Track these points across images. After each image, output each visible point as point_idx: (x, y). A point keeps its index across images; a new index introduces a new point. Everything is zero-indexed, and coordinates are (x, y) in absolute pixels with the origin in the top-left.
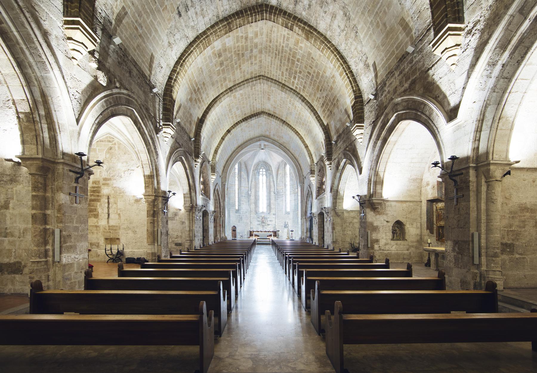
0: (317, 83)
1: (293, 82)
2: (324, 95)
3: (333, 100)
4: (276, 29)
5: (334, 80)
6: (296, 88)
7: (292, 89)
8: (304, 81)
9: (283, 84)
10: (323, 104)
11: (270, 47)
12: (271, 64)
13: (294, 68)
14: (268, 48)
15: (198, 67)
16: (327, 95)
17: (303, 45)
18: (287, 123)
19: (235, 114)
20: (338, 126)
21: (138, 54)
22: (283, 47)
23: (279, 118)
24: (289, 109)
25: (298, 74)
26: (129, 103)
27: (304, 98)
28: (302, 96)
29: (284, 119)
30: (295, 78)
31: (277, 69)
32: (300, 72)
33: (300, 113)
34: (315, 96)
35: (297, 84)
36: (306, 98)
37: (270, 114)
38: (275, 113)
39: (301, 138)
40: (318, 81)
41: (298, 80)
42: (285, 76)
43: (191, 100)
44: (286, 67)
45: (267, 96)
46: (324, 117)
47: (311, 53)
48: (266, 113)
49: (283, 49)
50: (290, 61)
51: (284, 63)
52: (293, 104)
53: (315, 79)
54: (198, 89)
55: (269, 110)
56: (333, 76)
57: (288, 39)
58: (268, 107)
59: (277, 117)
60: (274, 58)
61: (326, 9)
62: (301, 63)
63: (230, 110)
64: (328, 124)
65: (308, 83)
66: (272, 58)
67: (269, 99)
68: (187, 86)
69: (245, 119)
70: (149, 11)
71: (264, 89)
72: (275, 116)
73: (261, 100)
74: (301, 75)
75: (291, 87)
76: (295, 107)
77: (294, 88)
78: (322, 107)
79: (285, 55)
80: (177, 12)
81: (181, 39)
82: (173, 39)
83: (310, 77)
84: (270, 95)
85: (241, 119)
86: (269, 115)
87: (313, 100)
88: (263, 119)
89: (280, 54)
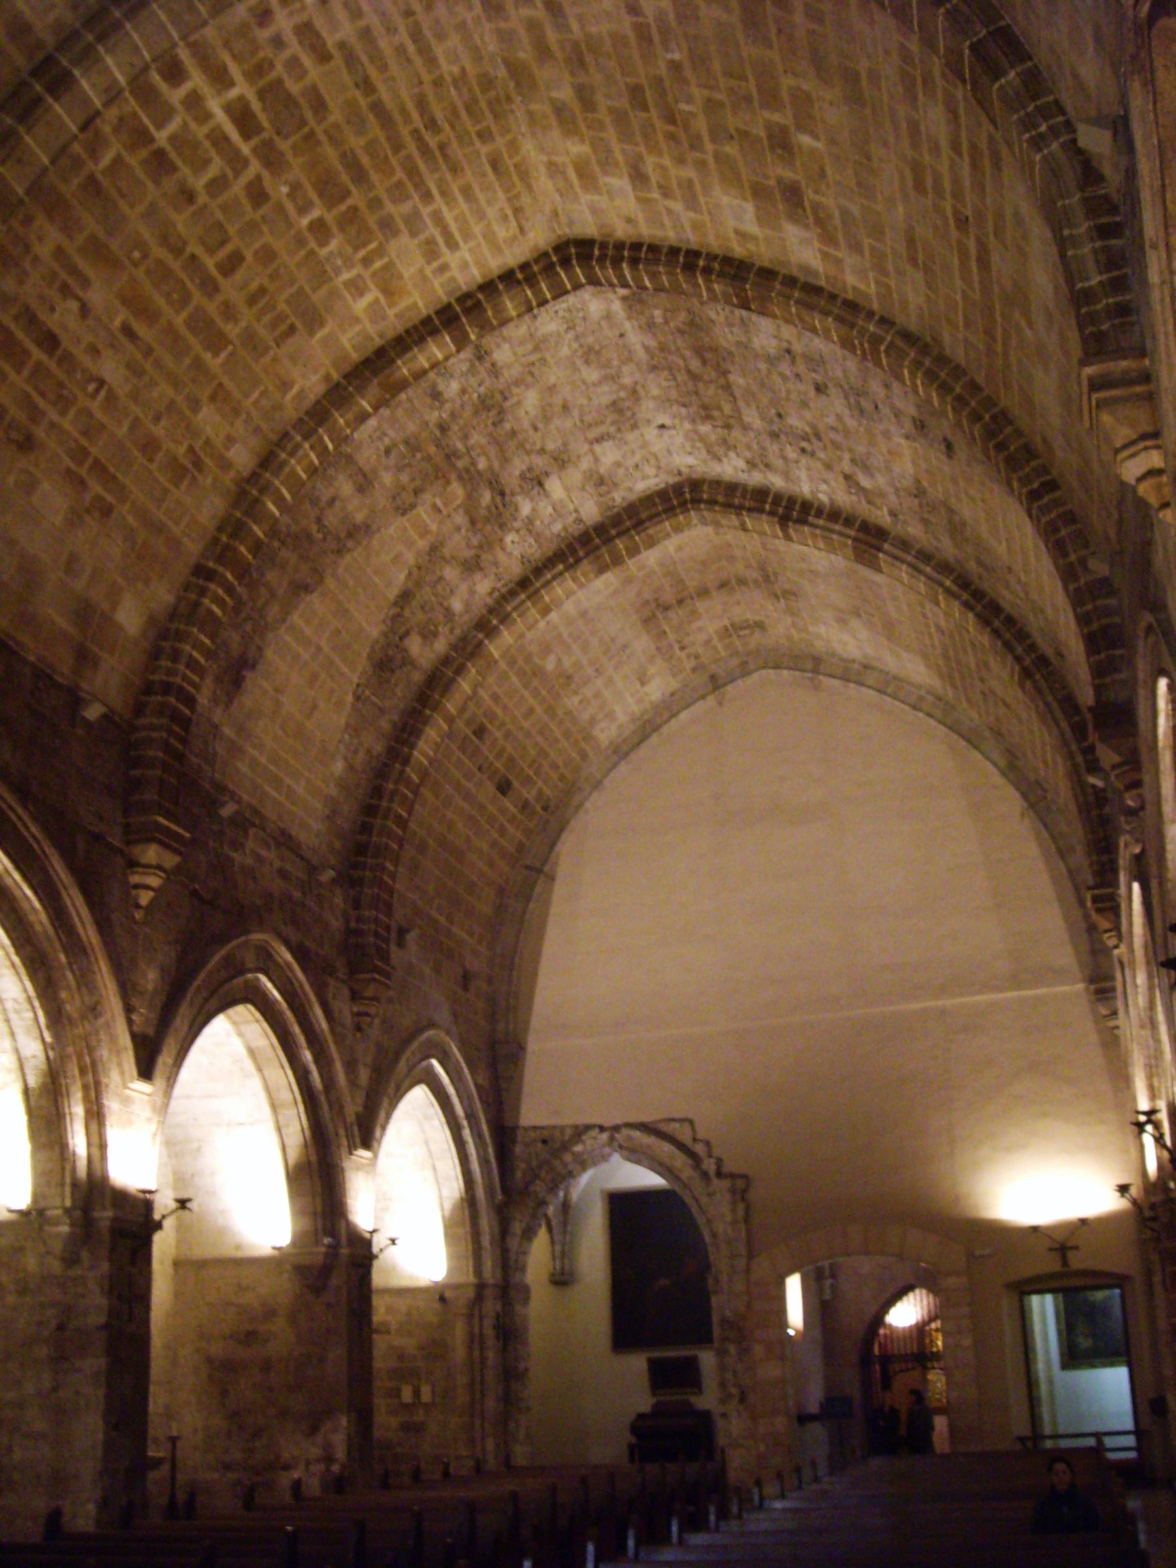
1: (221, 79)
2: (111, 369)
4: (502, 233)
8: (199, 183)
11: (485, 136)
12: (416, 35)
13: (297, 167)
14: (489, 119)
17: (360, 306)
22: (427, 196)
25: (255, 167)
30: (243, 117)
31: (366, 34)
32: (258, 194)
34: (97, 250)
35: (194, 102)
40: (179, 320)
41: (219, 139)
42: (294, 46)
44: (336, 115)
47: (311, 332)
49: (419, 185)
50: (345, 178)
51: (360, 126)
53: (197, 297)
57: (431, 252)
60: (428, 89)
61: (392, 461)
62: (301, 242)
65: (181, 221)
66: (438, 83)
74: (238, 188)
79: (384, 167)
83: (210, 263)
89: (412, 147)
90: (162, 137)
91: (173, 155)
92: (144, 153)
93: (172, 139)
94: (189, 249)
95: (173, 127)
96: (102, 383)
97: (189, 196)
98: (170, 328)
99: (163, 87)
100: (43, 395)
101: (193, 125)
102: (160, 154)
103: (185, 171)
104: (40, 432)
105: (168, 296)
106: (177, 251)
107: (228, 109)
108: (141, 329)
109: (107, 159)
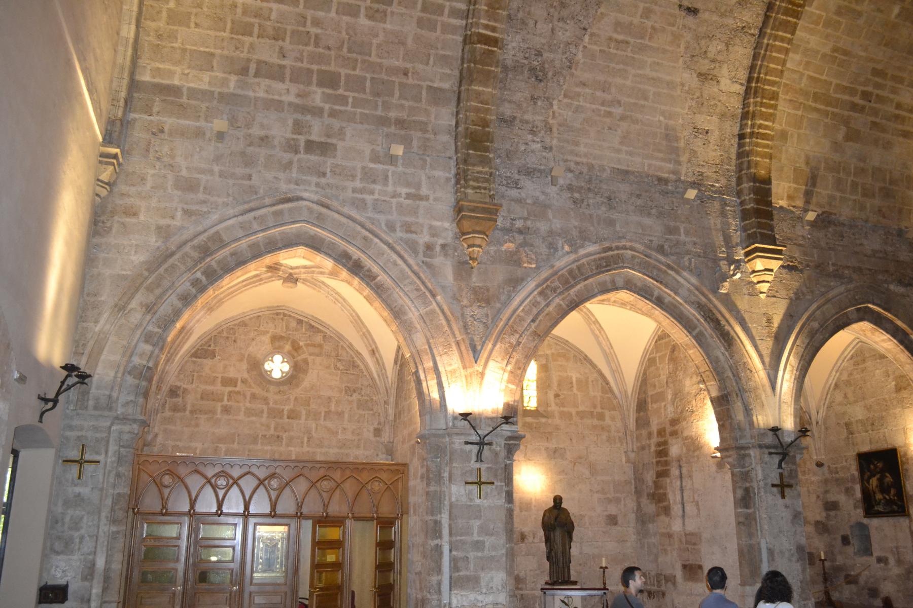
15: (824, 56)
21: (627, 153)
26: (606, 263)
43: (853, 136)
54: (866, 95)
68: (814, 116)
70: (621, 66)
80: (683, 13)
81: (727, 45)
82: (706, 61)
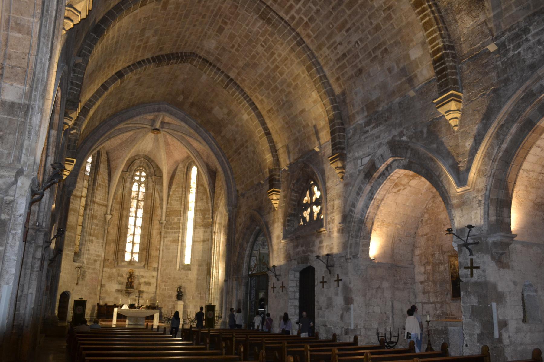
0: (346, 17)
1: (291, 7)
2: (355, 38)
3: (374, 50)
5: (390, 15)
6: (293, 18)
7: (282, 19)
8: (315, 8)
9: (268, 6)
10: (344, 55)
16: (361, 40)
18: (235, 83)
19: (147, 42)
20: (374, 98)
23: (223, 72)
24: (254, 57)
27: (301, 39)
28: (298, 34)
29: (232, 75)
33: (277, 67)
34: (329, 38)
35: (298, 12)
36: (305, 39)
37: (207, 61)
38: (219, 60)
39: (259, 115)
40: (348, 12)
45: (220, 24)
46: (338, 79)
48: (200, 57)
52: (270, 47)
55: (208, 53)
56: (389, 8)
58: (211, 44)
59: (219, 69)
63: (144, 30)
64: (343, 93)
65: (324, 13)
67: (220, 30)
69: (158, 60)
71: (220, 8)
72: (214, 66)
73: (203, 30)
75: (282, 14)
76: (273, 54)
77: (287, 18)
78: (338, 60)
84: (226, 23)
85: (149, 55)
86: (205, 61)
87: (319, 48)
88: (183, 70)
90: (306, 19)
91: (309, 16)
92: (310, 24)
93: (306, 17)
94: (331, 10)
95: (303, 17)
96: (357, 42)
97: (318, 10)
98: (350, 16)
99: (296, 20)
100: (353, 62)
101: (302, 12)
102: (309, 19)
103: (312, 13)
104: (360, 66)
105: (341, 17)
106: (331, 13)
107: (297, 4)
108: (348, 26)
109: (311, 33)
